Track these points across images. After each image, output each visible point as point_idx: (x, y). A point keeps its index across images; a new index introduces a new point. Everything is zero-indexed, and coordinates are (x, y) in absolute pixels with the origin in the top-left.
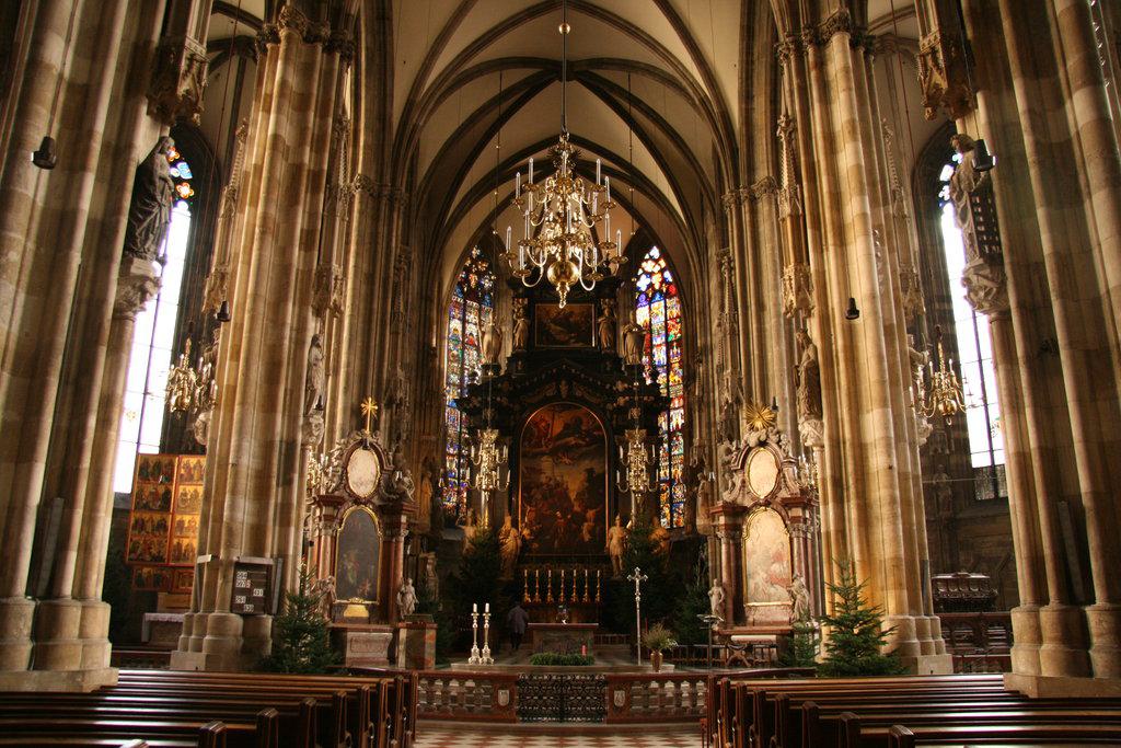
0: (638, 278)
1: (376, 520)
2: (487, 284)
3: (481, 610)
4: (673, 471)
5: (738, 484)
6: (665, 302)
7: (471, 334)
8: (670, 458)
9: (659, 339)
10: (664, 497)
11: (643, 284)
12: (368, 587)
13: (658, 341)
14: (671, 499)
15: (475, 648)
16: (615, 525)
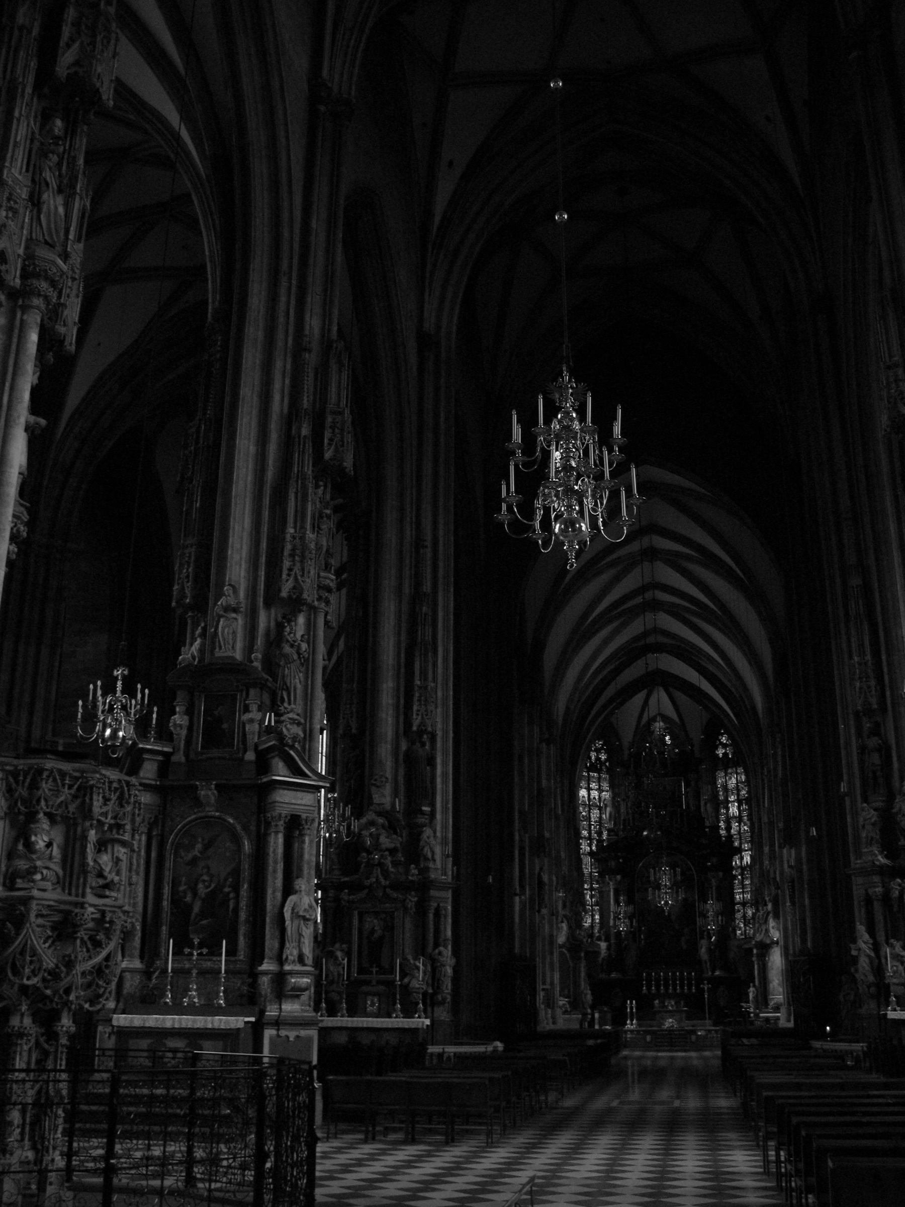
0: (716, 748)
1: (568, 955)
2: (603, 757)
3: (631, 1003)
4: (745, 896)
5: (764, 931)
6: (736, 769)
7: (594, 798)
8: (743, 886)
9: (732, 797)
10: (739, 915)
11: (720, 752)
12: (566, 992)
13: (732, 798)
14: (744, 916)
15: (628, 1022)
16: (704, 938)
